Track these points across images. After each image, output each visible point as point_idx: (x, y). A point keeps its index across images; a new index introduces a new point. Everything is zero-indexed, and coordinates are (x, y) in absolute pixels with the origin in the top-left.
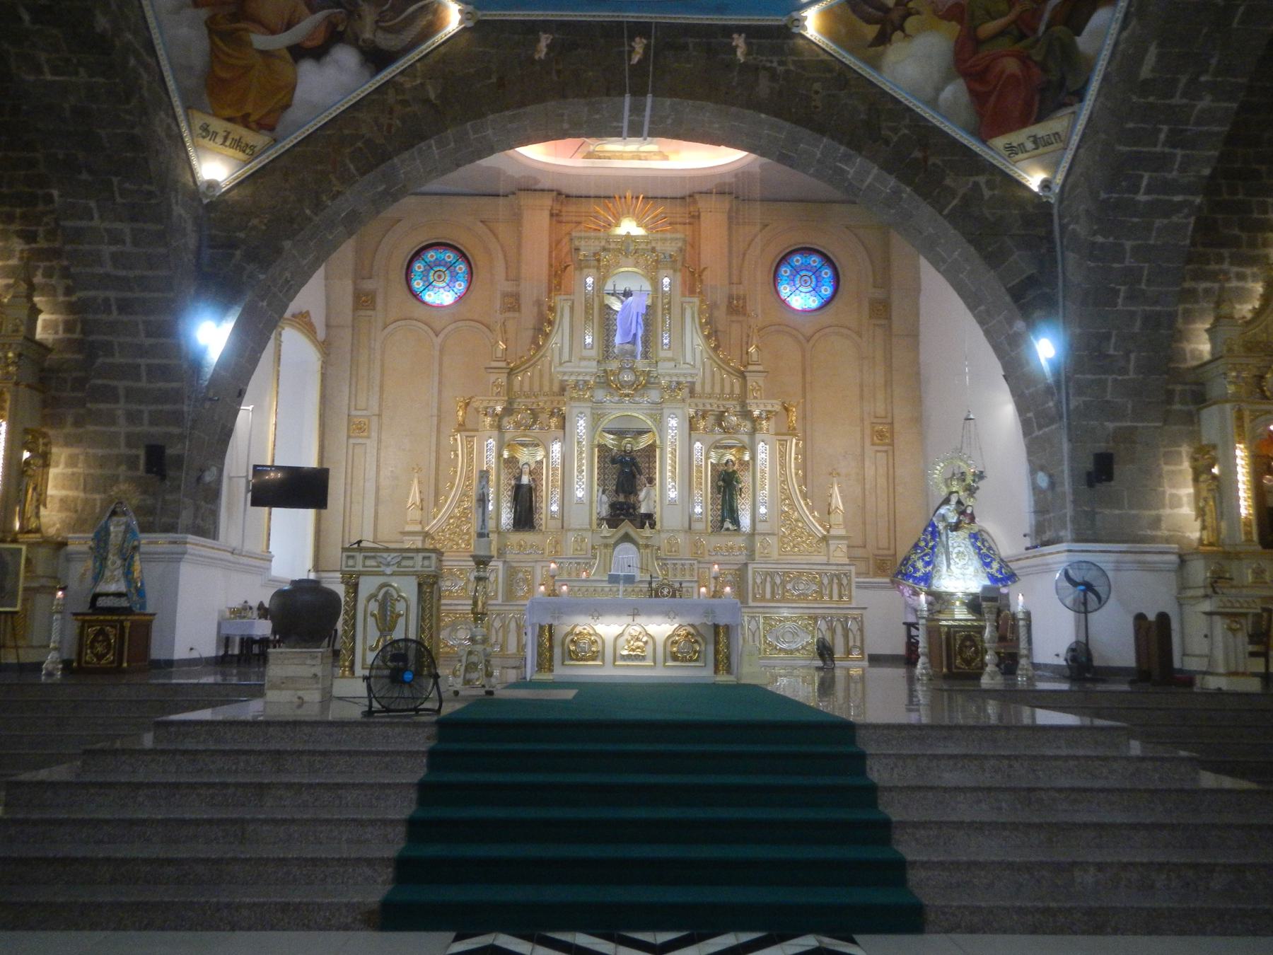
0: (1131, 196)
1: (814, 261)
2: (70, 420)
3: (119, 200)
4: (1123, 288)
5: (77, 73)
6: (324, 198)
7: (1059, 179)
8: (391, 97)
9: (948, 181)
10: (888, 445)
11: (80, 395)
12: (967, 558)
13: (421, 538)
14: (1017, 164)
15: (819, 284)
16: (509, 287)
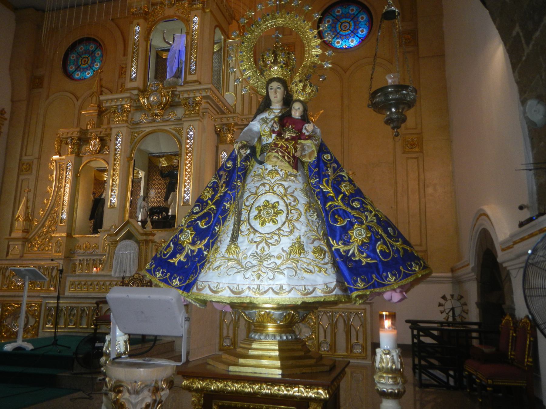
1: (352, 10)
10: (417, 152)
12: (281, 218)
13: (20, 243)
15: (357, 27)
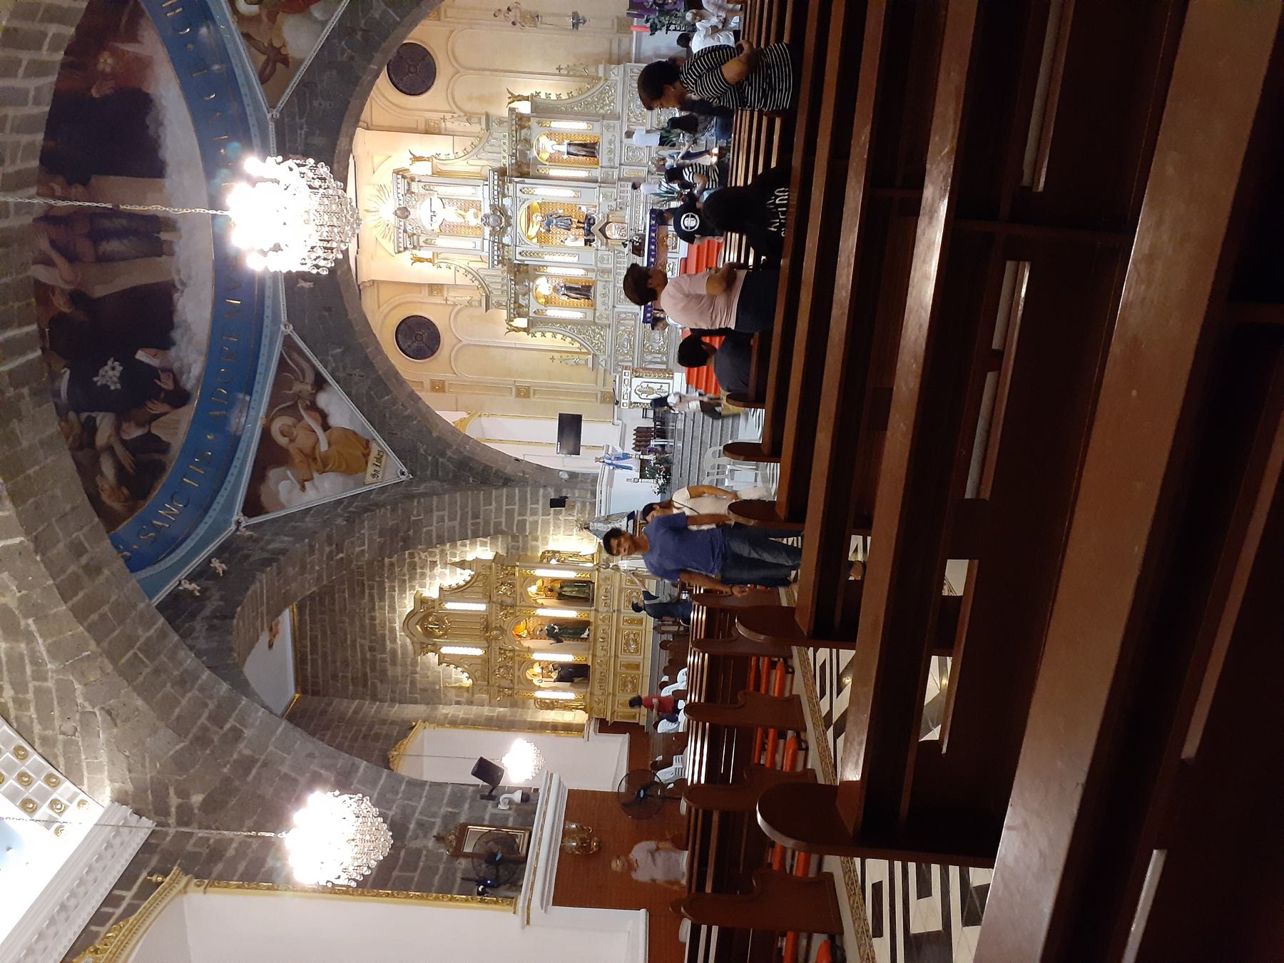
2: (534, 543)
5: (363, 534)
6: (406, 413)
8: (341, 375)
9: (377, 16)
11: (521, 538)
16: (426, 291)
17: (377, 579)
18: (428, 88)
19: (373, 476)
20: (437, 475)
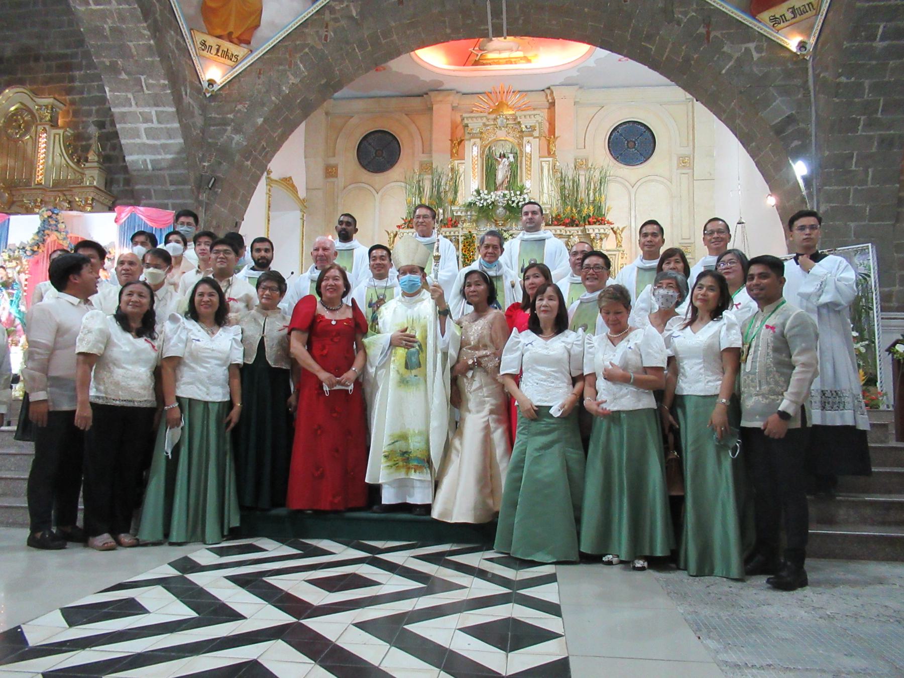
0: (869, 43)
3: (146, 92)
4: (863, 118)
7: (812, 41)
8: (327, 16)
9: (725, 49)
14: (780, 32)
16: (424, 158)
17: (84, 63)
18: (616, 158)
19: (204, 44)
20: (210, 125)
